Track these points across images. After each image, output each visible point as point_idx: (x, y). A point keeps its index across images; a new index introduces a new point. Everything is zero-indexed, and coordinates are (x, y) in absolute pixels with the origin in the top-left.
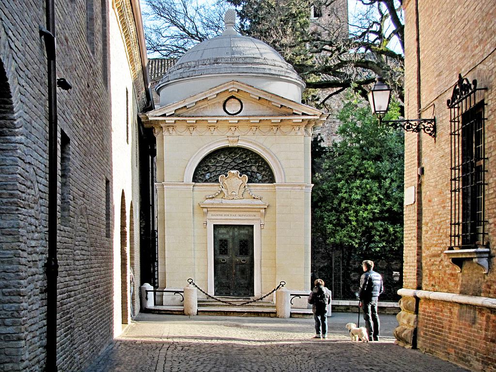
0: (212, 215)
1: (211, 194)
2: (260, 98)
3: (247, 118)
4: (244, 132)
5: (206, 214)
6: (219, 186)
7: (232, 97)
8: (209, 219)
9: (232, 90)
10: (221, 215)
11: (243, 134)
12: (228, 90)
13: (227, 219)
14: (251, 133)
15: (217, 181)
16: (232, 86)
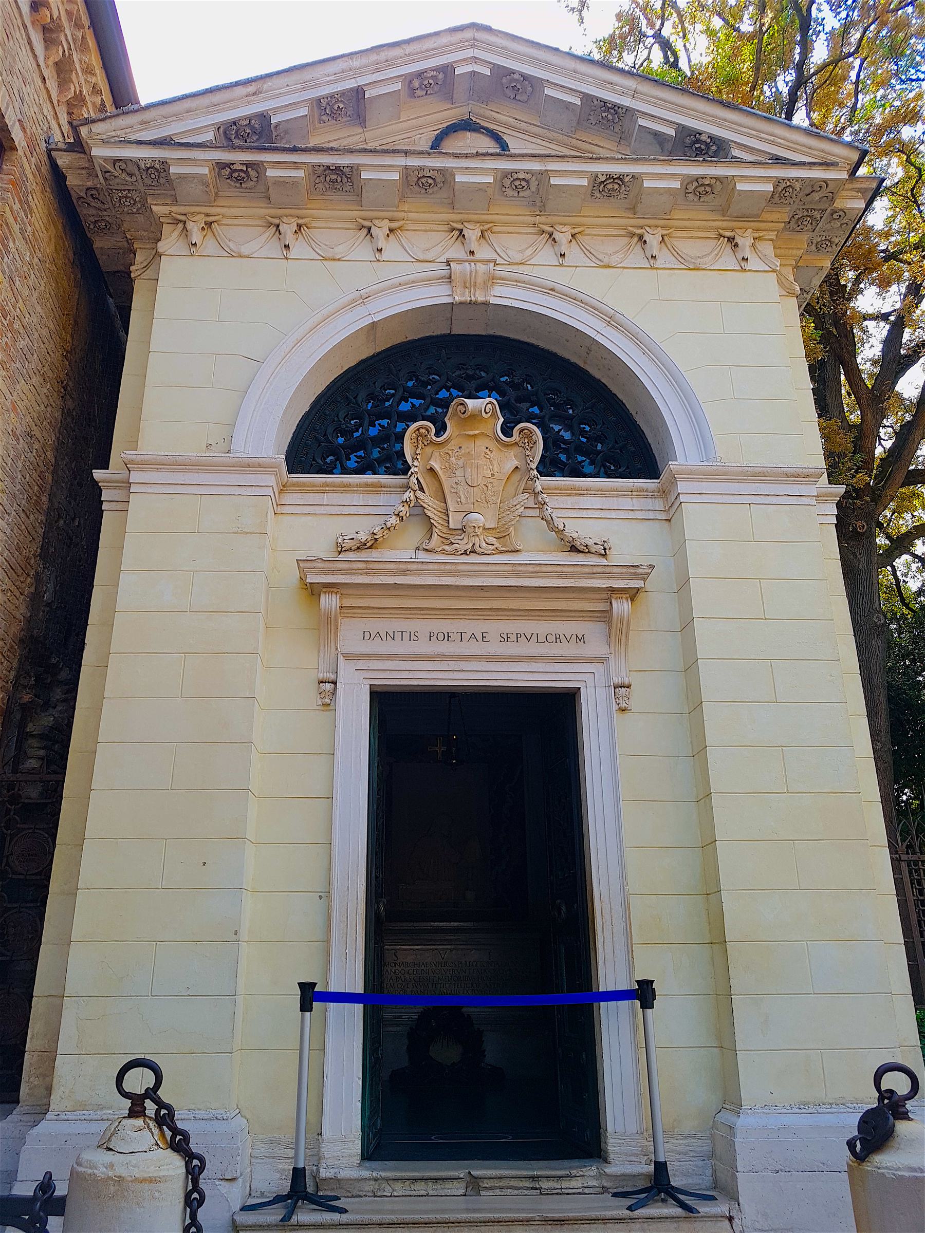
0: (367, 636)
1: (362, 529)
2: (586, 97)
3: (536, 166)
4: (522, 252)
5: (327, 626)
6: (408, 487)
7: (467, 126)
8: (347, 656)
9: (469, 68)
10: (414, 636)
11: (518, 258)
12: (447, 70)
13: (442, 657)
14: (547, 255)
15: (396, 464)
16: (469, 53)
